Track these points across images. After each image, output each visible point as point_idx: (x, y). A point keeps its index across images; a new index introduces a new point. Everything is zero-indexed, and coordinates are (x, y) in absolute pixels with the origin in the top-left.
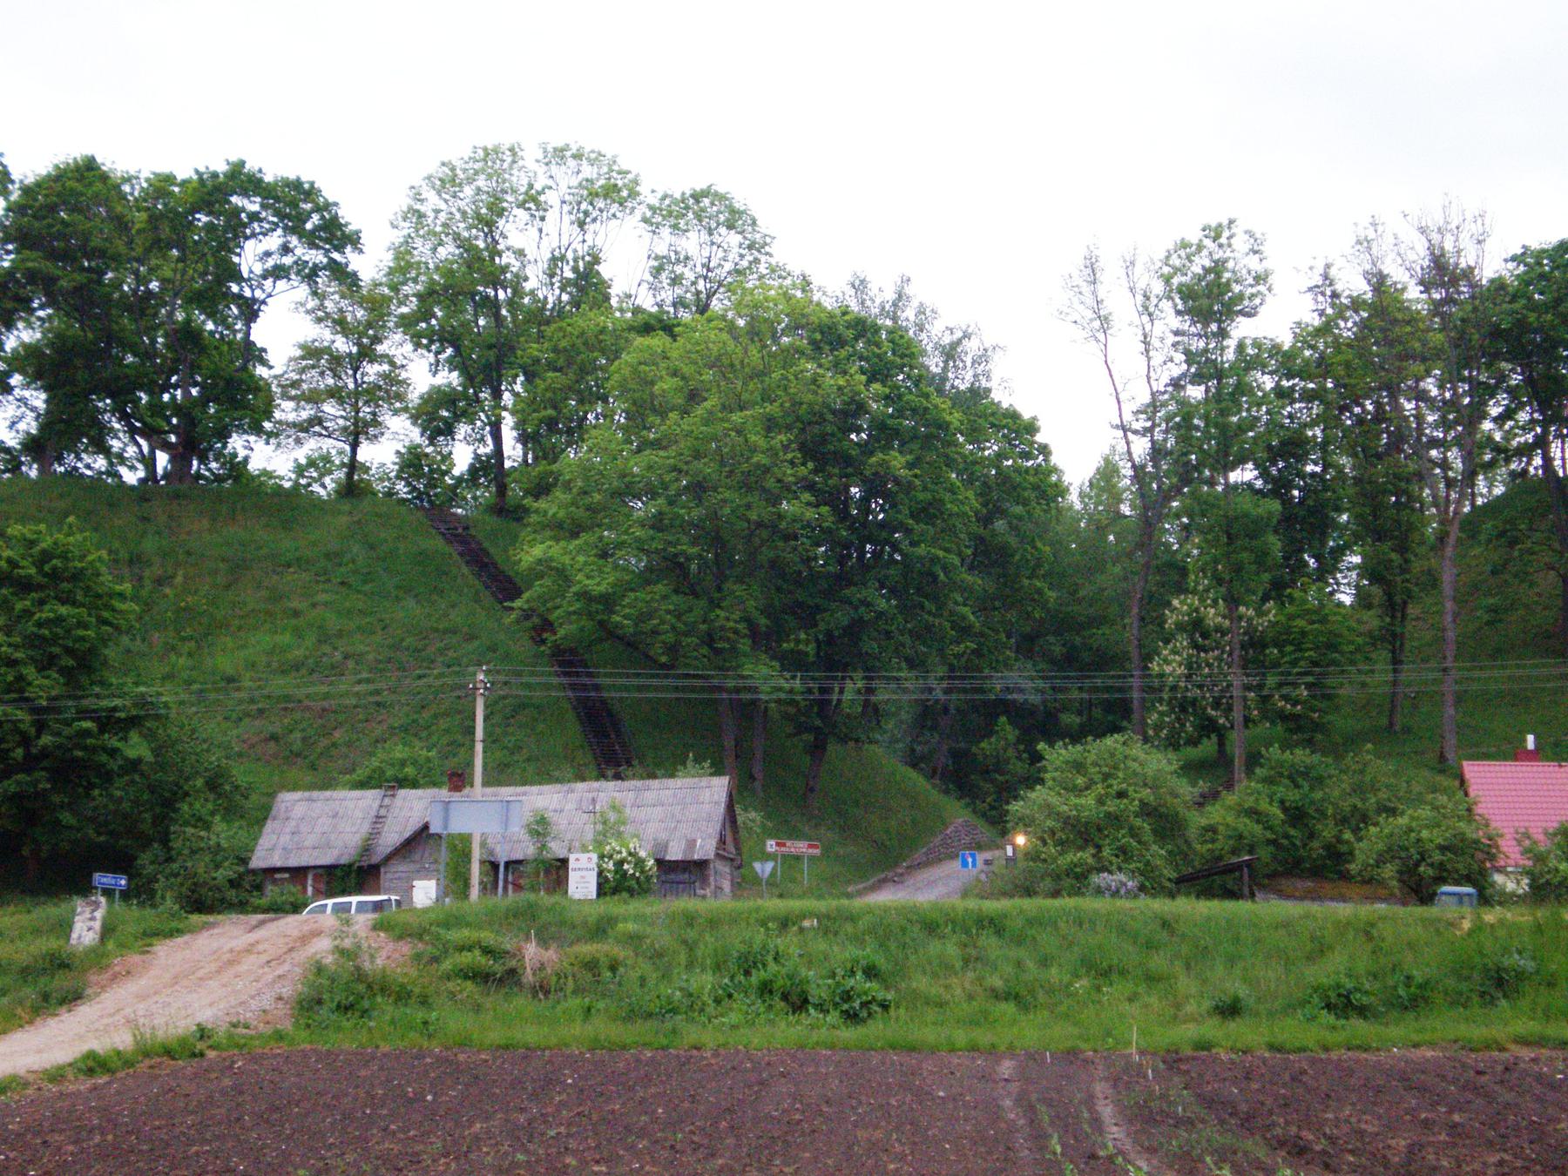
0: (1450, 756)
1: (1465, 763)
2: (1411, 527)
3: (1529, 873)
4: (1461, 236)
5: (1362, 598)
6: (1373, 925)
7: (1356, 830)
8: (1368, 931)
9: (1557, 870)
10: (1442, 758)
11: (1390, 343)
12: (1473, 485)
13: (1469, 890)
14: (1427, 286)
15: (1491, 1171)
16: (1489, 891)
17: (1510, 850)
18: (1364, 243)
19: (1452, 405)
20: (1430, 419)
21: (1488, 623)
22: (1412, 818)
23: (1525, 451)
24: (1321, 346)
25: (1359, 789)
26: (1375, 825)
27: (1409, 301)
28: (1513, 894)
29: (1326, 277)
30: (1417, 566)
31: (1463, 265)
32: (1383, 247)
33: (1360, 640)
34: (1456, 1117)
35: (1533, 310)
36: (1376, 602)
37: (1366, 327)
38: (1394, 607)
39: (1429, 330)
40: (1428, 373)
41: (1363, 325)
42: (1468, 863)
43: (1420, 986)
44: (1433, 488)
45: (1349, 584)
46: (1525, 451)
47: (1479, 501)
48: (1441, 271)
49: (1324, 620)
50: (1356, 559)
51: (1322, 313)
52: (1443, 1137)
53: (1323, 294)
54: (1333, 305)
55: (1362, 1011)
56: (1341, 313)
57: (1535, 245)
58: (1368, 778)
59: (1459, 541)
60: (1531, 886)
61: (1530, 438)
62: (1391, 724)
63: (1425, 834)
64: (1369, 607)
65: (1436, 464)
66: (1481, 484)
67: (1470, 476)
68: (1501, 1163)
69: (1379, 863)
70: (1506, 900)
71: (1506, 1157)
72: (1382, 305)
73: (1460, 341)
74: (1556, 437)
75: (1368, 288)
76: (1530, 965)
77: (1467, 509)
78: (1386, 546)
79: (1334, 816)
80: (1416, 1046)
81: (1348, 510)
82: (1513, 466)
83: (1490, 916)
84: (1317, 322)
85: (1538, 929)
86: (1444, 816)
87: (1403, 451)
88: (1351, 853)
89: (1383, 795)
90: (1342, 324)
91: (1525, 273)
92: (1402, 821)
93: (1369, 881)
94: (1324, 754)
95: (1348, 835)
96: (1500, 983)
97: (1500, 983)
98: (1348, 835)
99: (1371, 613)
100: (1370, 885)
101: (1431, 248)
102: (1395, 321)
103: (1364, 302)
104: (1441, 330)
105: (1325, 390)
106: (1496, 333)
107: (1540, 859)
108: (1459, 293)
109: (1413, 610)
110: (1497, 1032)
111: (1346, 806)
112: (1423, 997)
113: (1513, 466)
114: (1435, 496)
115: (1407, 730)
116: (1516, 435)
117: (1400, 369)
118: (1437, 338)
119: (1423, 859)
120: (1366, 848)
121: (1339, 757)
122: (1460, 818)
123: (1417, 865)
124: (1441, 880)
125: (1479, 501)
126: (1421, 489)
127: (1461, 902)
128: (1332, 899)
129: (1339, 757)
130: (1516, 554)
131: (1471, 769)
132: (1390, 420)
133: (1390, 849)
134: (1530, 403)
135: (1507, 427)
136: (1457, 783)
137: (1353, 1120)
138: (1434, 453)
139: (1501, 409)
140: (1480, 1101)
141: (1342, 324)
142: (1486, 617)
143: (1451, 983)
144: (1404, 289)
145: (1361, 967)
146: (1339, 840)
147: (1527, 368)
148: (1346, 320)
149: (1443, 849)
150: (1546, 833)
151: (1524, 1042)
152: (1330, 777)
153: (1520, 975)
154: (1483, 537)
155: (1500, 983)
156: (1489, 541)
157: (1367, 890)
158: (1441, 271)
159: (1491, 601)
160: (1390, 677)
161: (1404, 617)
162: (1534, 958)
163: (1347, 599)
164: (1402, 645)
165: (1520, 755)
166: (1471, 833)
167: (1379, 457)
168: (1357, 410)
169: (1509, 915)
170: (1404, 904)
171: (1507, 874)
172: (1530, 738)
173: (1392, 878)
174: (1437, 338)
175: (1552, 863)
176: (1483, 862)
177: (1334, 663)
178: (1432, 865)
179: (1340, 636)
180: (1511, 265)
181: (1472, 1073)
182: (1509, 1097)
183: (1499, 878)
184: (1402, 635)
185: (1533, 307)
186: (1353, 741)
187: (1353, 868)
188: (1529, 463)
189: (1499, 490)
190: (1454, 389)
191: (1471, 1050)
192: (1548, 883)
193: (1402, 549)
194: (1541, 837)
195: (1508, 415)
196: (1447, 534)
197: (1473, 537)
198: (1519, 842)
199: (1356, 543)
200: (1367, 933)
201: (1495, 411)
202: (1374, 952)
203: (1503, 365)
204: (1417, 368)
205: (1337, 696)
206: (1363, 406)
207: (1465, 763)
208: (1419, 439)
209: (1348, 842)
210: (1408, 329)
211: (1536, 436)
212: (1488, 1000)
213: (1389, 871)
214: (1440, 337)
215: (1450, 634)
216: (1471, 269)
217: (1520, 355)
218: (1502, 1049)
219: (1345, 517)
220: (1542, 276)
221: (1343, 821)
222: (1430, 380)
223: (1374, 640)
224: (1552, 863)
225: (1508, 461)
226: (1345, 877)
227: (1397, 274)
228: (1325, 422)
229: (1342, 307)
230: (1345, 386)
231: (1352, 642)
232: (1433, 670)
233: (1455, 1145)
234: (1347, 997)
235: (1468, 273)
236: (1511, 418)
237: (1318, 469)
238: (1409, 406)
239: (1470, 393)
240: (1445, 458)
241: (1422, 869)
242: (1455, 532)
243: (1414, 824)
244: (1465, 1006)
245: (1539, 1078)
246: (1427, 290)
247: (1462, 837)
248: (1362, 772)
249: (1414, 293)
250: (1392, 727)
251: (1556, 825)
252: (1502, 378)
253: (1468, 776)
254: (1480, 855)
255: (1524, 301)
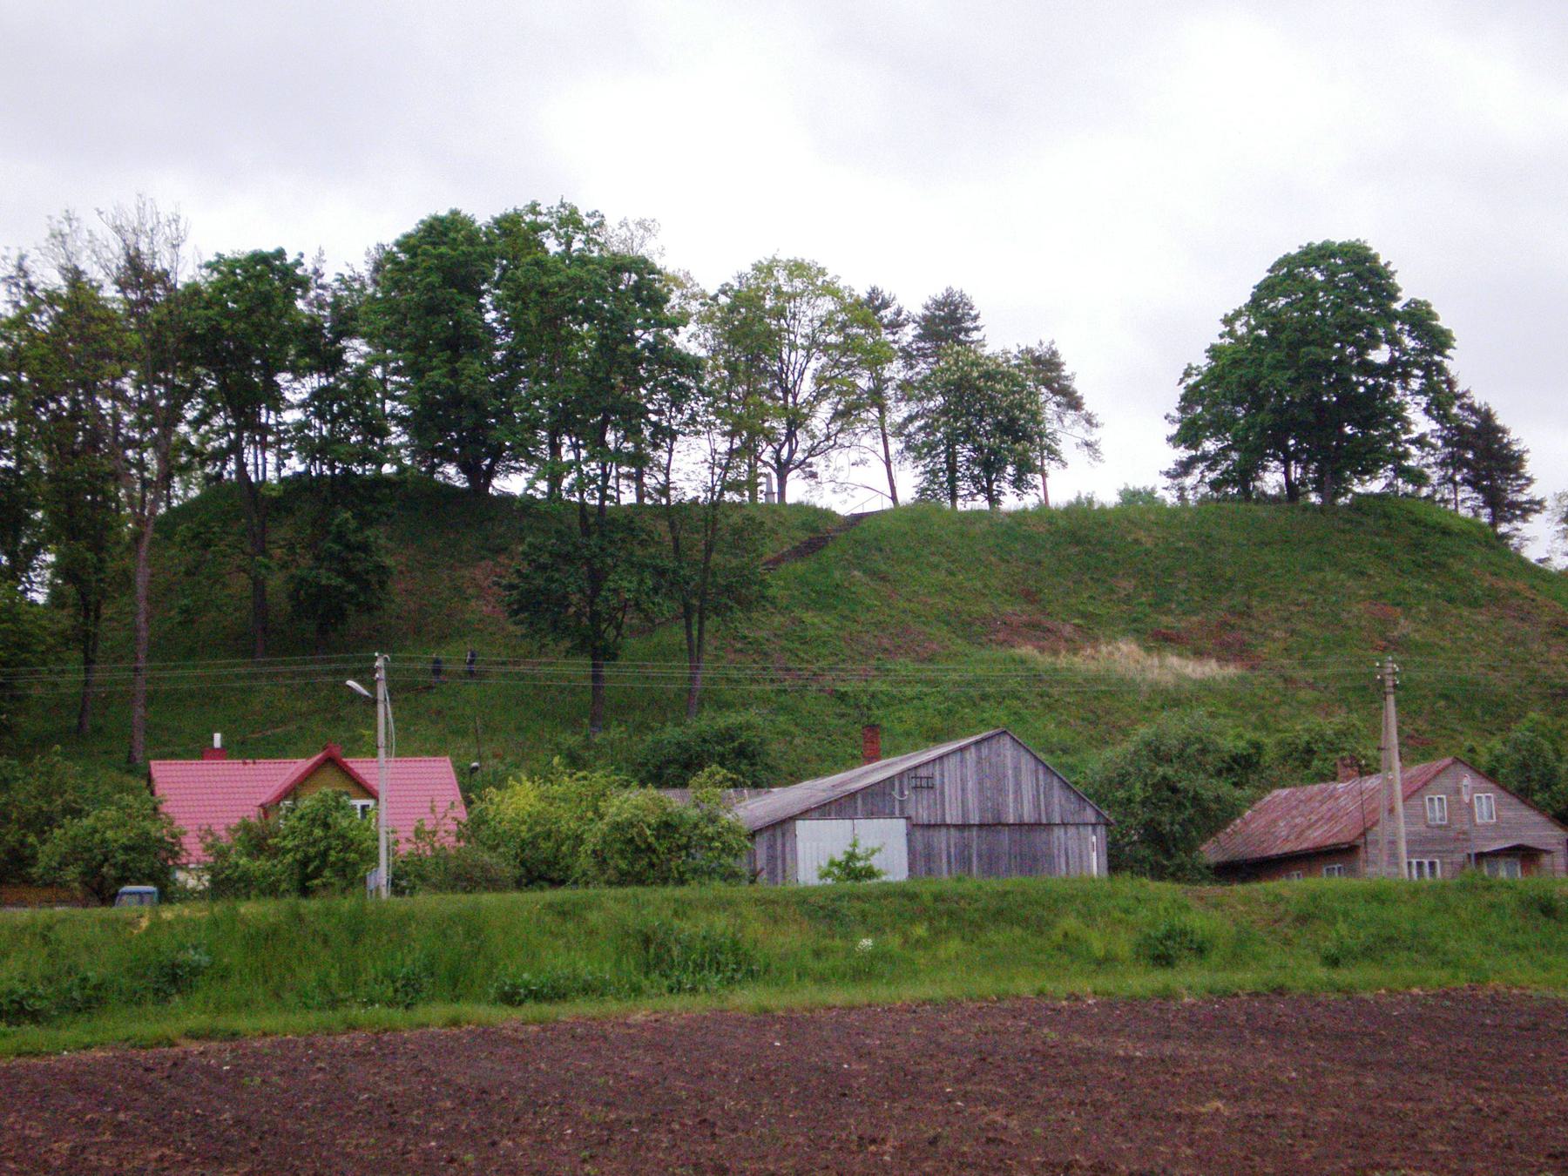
0: (138, 755)
1: (152, 763)
2: (107, 526)
3: (209, 869)
4: (156, 238)
5: (56, 597)
6: (50, 928)
7: (40, 833)
8: (45, 936)
9: (237, 865)
10: (131, 759)
11: (86, 340)
12: (169, 487)
13: (151, 888)
14: (123, 286)
15: (150, 1168)
16: (171, 889)
17: (193, 847)
18: (59, 237)
19: (149, 406)
20: (126, 419)
21: (180, 623)
22: (98, 819)
23: (221, 456)
24: (15, 338)
25: (46, 793)
26: (60, 827)
27: (106, 299)
28: (194, 891)
29: (20, 268)
30: (112, 566)
31: (158, 267)
32: (79, 242)
33: (50, 640)
34: (121, 1116)
35: (227, 318)
36: (70, 601)
37: (61, 322)
38: (88, 607)
39: (124, 330)
40: (125, 373)
41: (59, 319)
42: (151, 862)
43: (97, 987)
44: (129, 488)
45: (42, 583)
46: (221, 456)
47: (175, 503)
48: (137, 273)
49: (15, 619)
50: (50, 558)
51: (16, 305)
52: (107, 1137)
53: (17, 285)
54: (28, 298)
55: (35, 1017)
56: (36, 305)
57: (228, 254)
58: (54, 780)
59: (153, 543)
60: (211, 881)
61: (224, 442)
62: (81, 725)
63: (110, 834)
64: (63, 606)
65: (133, 465)
66: (177, 483)
67: (166, 479)
68: (162, 1158)
69: (63, 864)
70: (187, 896)
71: (168, 1152)
72: (78, 299)
73: (156, 343)
74: (248, 443)
75: (62, 283)
76: (205, 960)
77: (162, 510)
78: (80, 545)
79: (18, 820)
80: (87, 1047)
81: (42, 507)
82: (208, 470)
83: (168, 914)
84: (11, 313)
85: (215, 923)
86: (130, 816)
87: (100, 450)
88: (34, 857)
89: (69, 797)
90: (37, 318)
91: (219, 281)
92: (87, 822)
93: (49, 885)
94: (10, 756)
95: (32, 839)
96: (174, 979)
97: (174, 979)
98: (32, 839)
99: (65, 612)
100: (52, 888)
101: (127, 247)
102: (91, 318)
103: (60, 296)
104: (137, 331)
105: (21, 384)
106: (192, 338)
107: (222, 854)
108: (153, 294)
109: (107, 611)
110: (170, 1028)
111: (31, 809)
112: (97, 999)
113: (208, 470)
114: (129, 496)
115: (99, 731)
116: (211, 439)
117: (97, 368)
118: (134, 339)
119: (106, 860)
120: (47, 854)
121: (26, 759)
122: (145, 818)
123: (101, 866)
124: (124, 880)
125: (175, 503)
126: (118, 490)
127: (141, 902)
128: (12, 905)
129: (26, 759)
130: (209, 556)
131: (158, 768)
132: (86, 418)
133: (74, 851)
134: (224, 409)
135: (202, 431)
136: (144, 783)
137: (18, 1127)
138: (130, 453)
139: (195, 413)
140: (146, 1098)
141: (37, 318)
142: (179, 619)
143: (125, 982)
144: (100, 287)
145: (35, 973)
146: (22, 844)
147: (221, 374)
148: (40, 313)
149: (127, 849)
150: (228, 829)
151: (193, 1035)
152: (16, 779)
153: (196, 971)
154: (177, 539)
155: (174, 979)
156: (184, 542)
157: (46, 894)
158: (137, 273)
159: (186, 601)
160: (82, 677)
161: (97, 618)
162: (209, 952)
163: (40, 597)
164: (95, 644)
165: (207, 753)
166: (154, 830)
167: (75, 454)
168: (52, 406)
169: (186, 912)
170: (86, 906)
171: (189, 871)
172: (217, 737)
173: (74, 880)
174: (134, 339)
175: (233, 858)
176: (166, 860)
177: (25, 663)
178: (114, 866)
179: (31, 635)
180: (205, 272)
181: (141, 1071)
182: (173, 1091)
183: (181, 876)
184: (95, 635)
185: (229, 314)
186: (41, 743)
187: (35, 871)
188: (223, 467)
189: (194, 493)
190: (151, 391)
191: (142, 1047)
192: (228, 878)
193: (98, 547)
194: (223, 833)
195: (203, 419)
196: (142, 534)
197: (168, 538)
198: (202, 840)
199: (50, 542)
200: (44, 937)
201: (191, 415)
202: (50, 955)
203: (198, 369)
204: (113, 367)
205: (28, 697)
206: (59, 402)
207: (152, 763)
208: (116, 439)
209: (32, 845)
210: (104, 327)
211: (230, 440)
212: (161, 996)
213: (72, 873)
214: (136, 337)
215: (143, 634)
216: (166, 273)
217: (215, 361)
218: (172, 1045)
219: (40, 514)
220: (236, 285)
221: (27, 824)
222: (126, 380)
223: (66, 639)
224: (233, 858)
225: (203, 464)
226: (28, 882)
227: (94, 272)
228: (19, 417)
229: (37, 301)
230: (40, 381)
231: (43, 642)
232: (125, 670)
233: (117, 1144)
234: (20, 1003)
235: (164, 276)
236: (206, 423)
237: (11, 464)
238: (106, 406)
239: (166, 396)
240: (142, 458)
241: (105, 870)
242: (150, 533)
243: (99, 825)
244: (138, 1004)
245: (207, 1070)
246: (123, 290)
247: (146, 835)
248: (49, 774)
249: (110, 292)
250: (83, 728)
251: (238, 821)
252: (197, 382)
253: (155, 775)
254: (164, 854)
255: (217, 309)
